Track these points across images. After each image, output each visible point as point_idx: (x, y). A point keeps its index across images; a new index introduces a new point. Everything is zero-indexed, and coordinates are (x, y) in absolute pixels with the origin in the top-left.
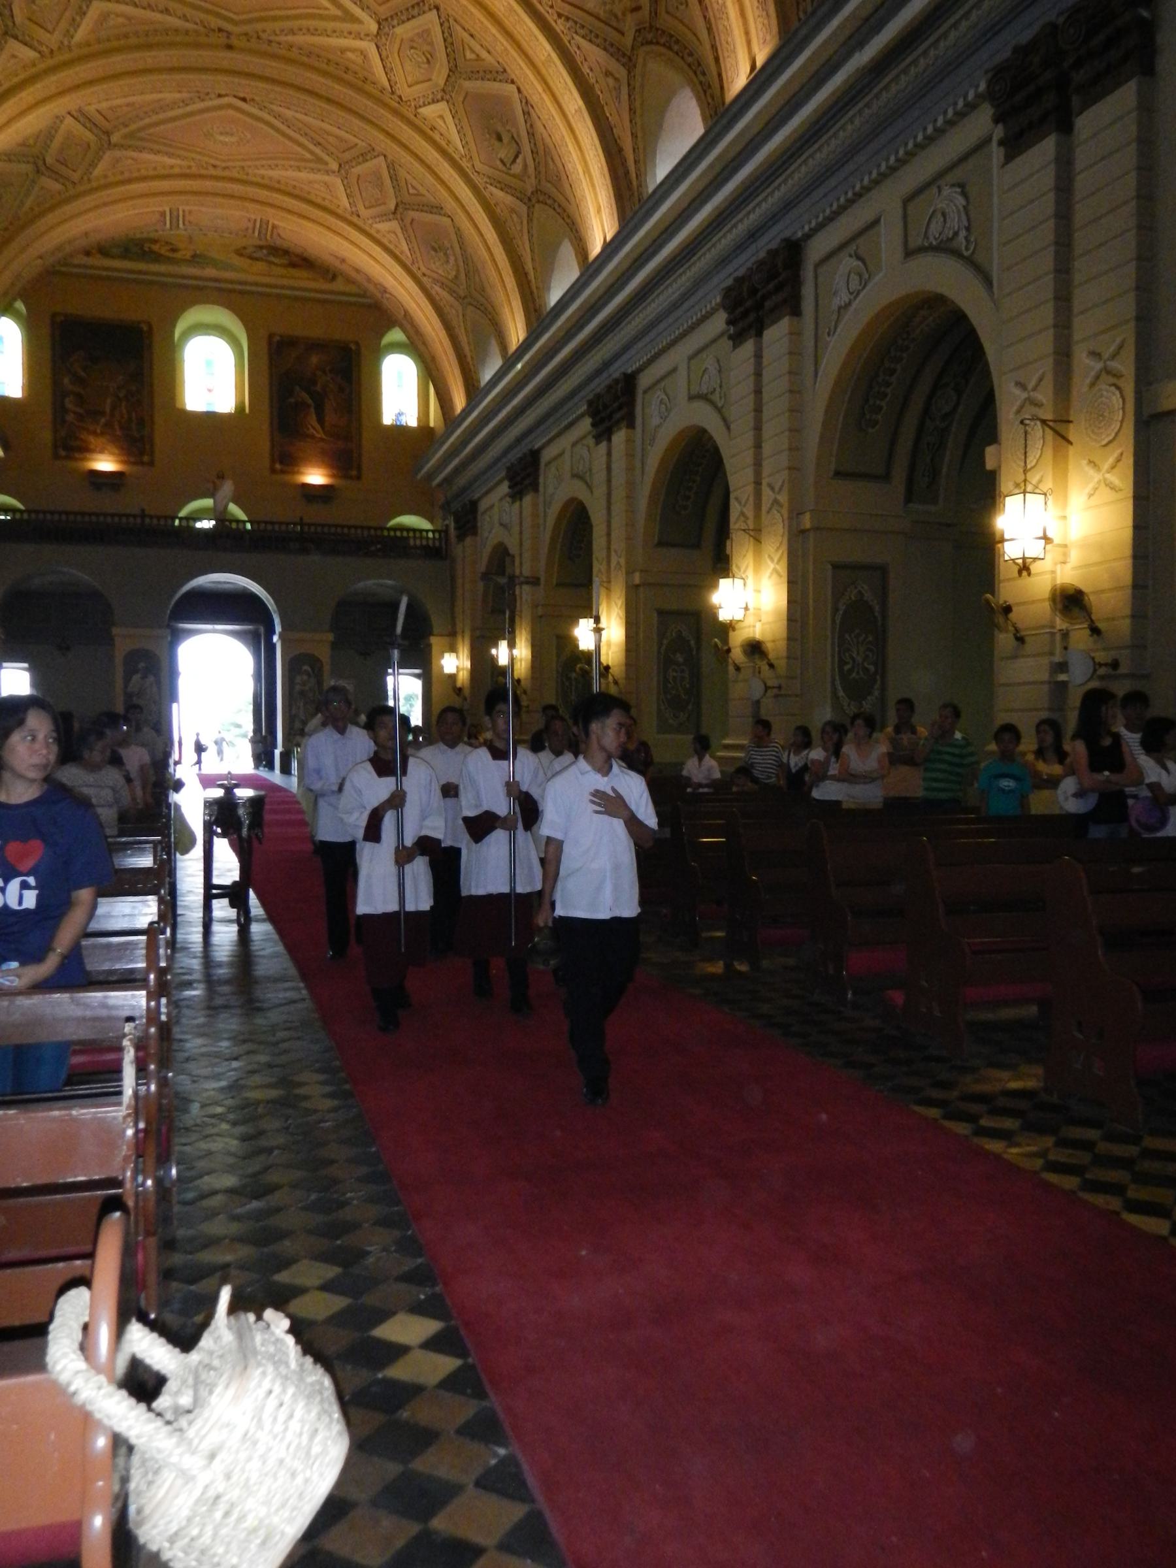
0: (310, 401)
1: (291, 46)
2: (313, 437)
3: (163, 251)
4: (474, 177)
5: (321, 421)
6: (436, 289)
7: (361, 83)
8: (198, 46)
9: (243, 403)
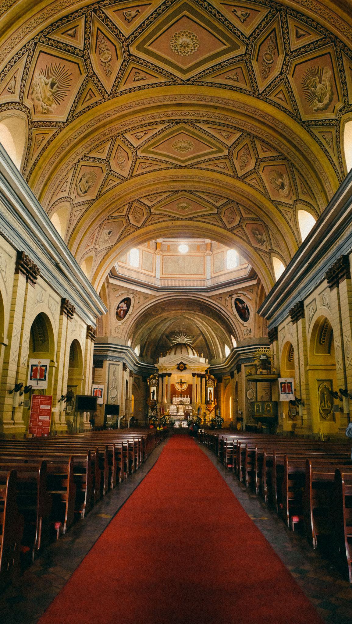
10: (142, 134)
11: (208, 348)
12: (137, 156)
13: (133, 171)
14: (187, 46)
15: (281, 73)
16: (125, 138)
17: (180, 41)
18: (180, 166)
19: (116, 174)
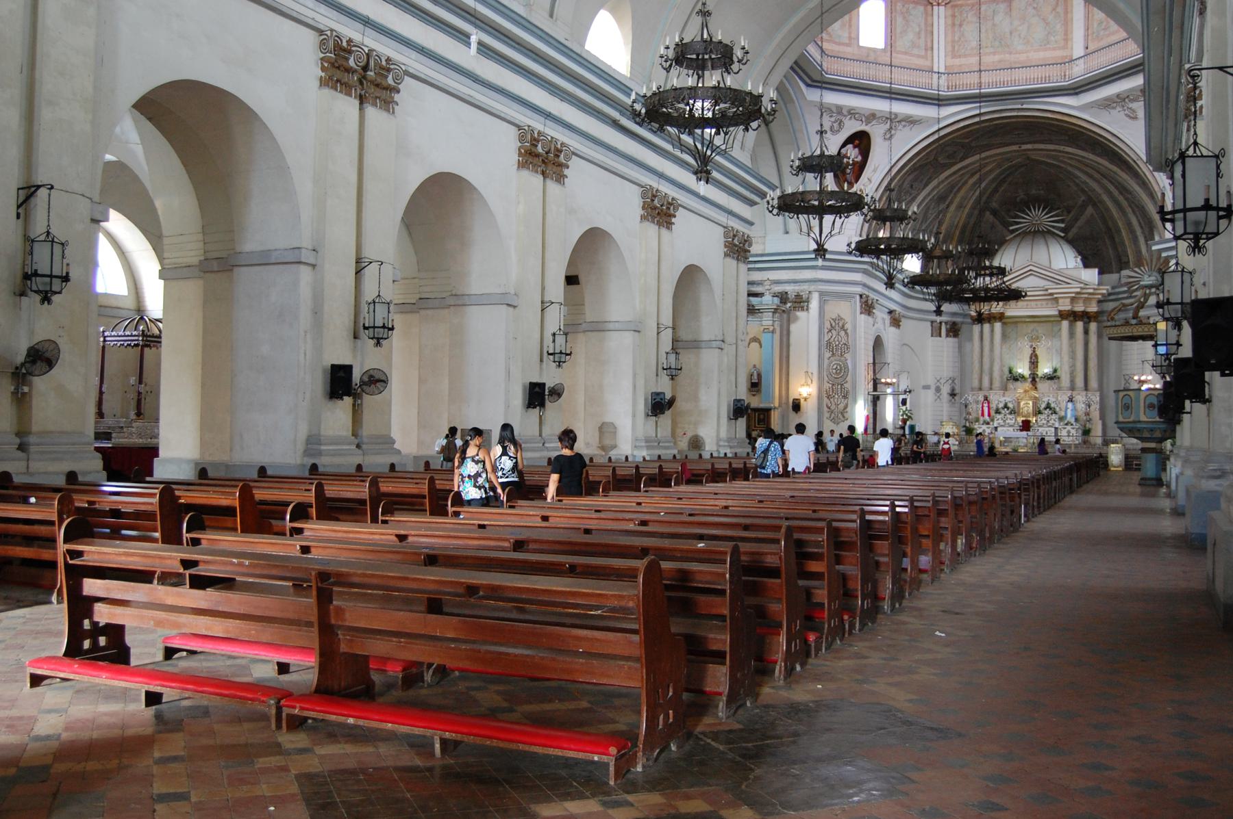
11: (1112, 238)
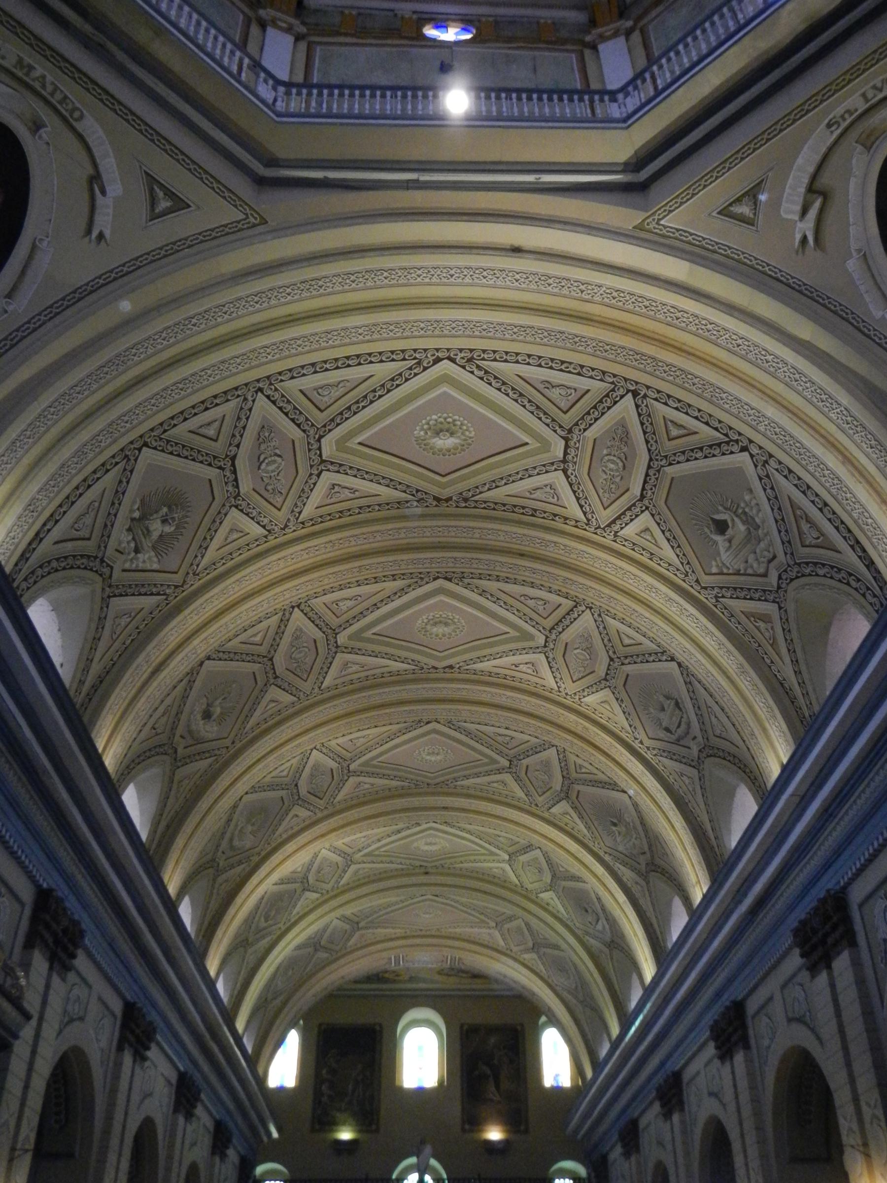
0: (489, 1072)
1: (461, 869)
2: (492, 1100)
3: (391, 976)
4: (576, 931)
5: (497, 1087)
6: (565, 994)
7: (503, 883)
8: (408, 875)
9: (443, 1076)
10: (523, 668)
12: (547, 637)
13: (568, 614)
14: (429, 754)
15: (296, 785)
16: (557, 683)
17: (439, 758)
18: (450, 580)
19: (606, 640)
